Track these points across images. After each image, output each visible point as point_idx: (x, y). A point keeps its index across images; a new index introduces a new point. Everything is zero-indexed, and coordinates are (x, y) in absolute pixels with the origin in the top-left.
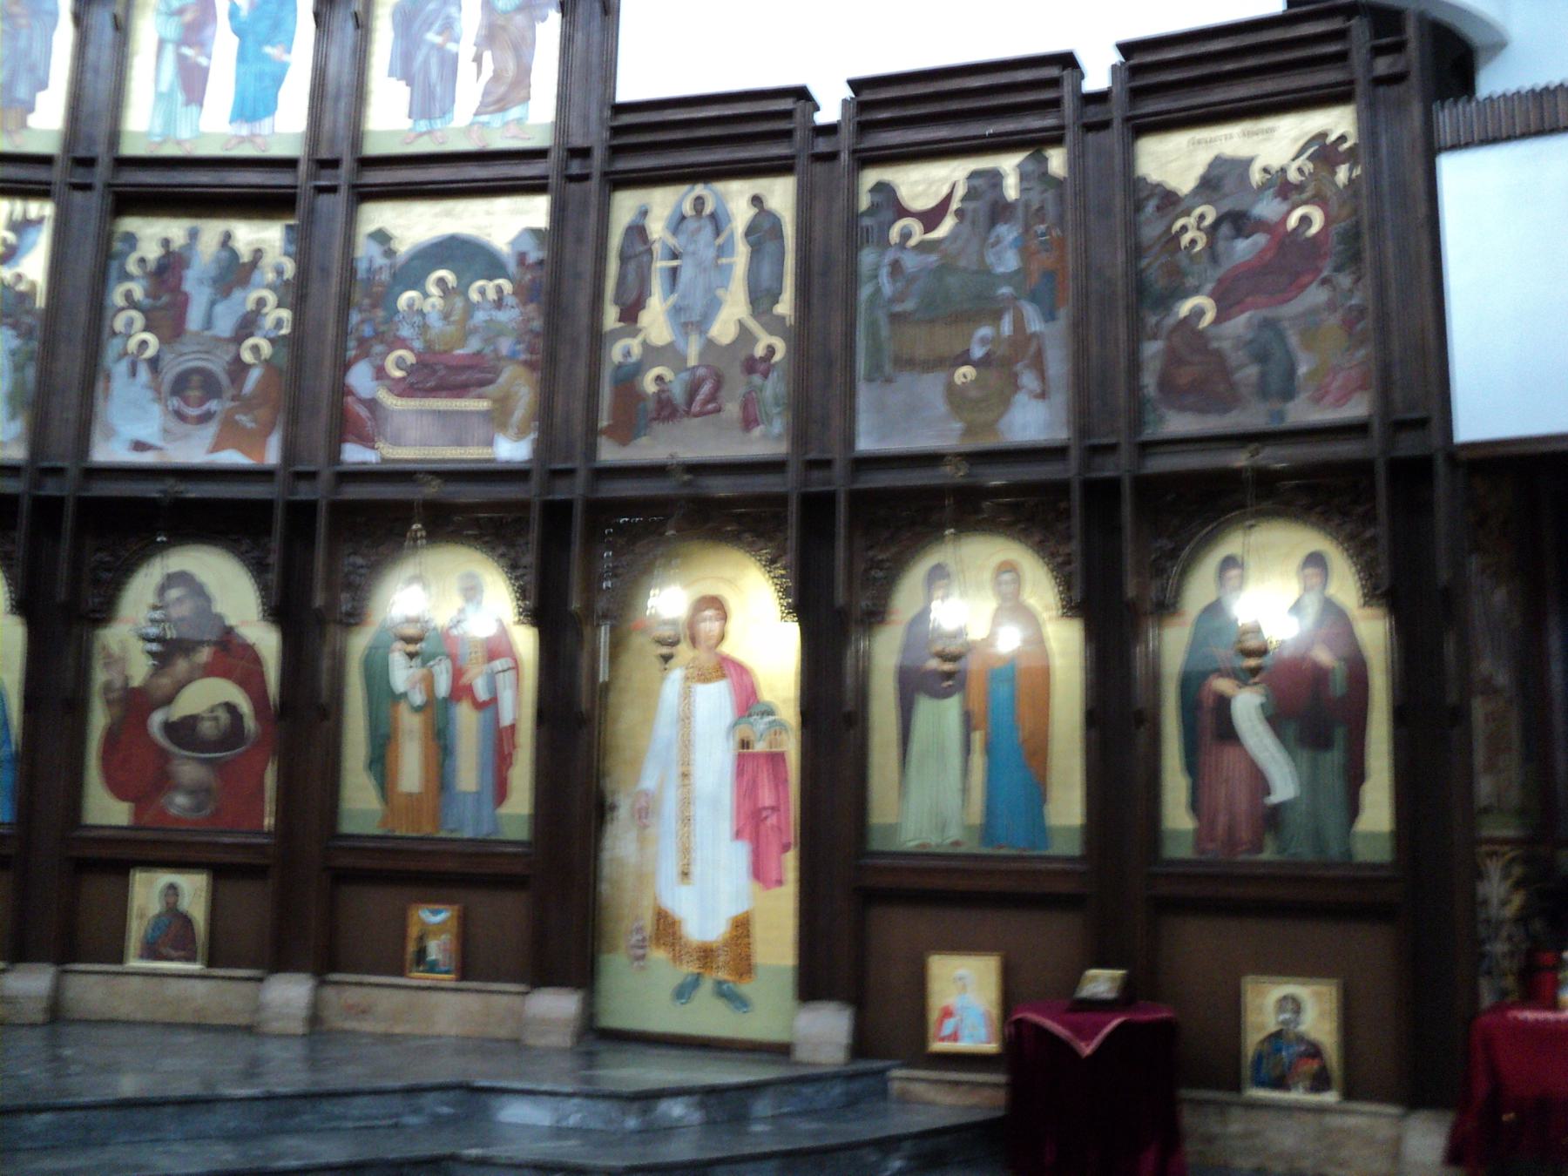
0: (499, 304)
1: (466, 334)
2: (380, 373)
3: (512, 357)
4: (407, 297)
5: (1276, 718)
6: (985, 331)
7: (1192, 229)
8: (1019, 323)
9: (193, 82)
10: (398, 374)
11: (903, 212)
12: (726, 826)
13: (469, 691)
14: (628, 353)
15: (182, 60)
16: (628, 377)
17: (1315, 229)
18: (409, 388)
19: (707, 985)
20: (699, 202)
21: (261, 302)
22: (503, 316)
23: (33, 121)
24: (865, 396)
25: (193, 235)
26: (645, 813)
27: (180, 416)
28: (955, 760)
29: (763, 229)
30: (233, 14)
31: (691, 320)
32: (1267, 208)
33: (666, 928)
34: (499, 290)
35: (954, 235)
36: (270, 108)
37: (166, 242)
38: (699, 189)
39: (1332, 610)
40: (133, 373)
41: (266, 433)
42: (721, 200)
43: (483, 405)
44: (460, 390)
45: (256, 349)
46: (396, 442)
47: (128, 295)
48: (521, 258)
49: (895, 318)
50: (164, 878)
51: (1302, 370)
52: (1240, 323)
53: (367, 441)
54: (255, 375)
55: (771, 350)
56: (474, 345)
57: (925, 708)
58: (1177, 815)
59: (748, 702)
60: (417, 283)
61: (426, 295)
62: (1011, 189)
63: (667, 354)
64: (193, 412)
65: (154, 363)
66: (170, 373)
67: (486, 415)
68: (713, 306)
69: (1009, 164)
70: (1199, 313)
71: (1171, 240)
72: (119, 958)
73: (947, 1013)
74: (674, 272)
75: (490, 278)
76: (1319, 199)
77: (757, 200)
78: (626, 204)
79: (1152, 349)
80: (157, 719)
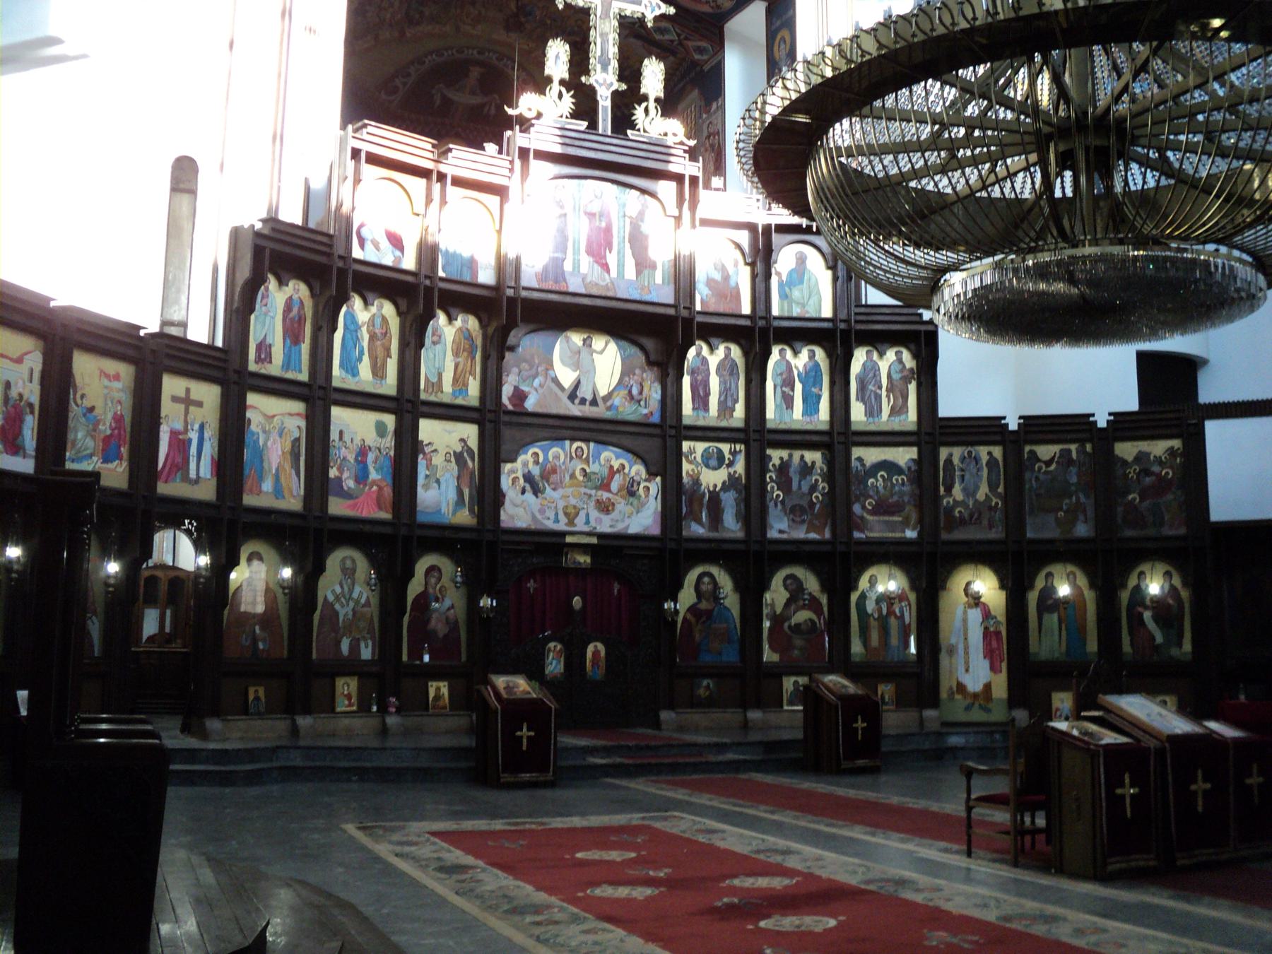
0: (903, 484)
1: (892, 495)
2: (864, 507)
3: (909, 501)
4: (871, 481)
5: (1156, 619)
6: (1067, 501)
7: (1132, 473)
8: (1078, 499)
9: (788, 401)
10: (870, 508)
11: (1039, 460)
12: (981, 655)
13: (894, 612)
14: (948, 502)
15: (783, 393)
16: (949, 511)
17: (1170, 476)
18: (874, 512)
19: (977, 705)
20: (970, 453)
21: (817, 481)
22: (905, 489)
23: (735, 414)
24: (1029, 520)
25: (791, 456)
26: (952, 651)
27: (793, 520)
28: (1056, 633)
29: (992, 462)
30: (799, 375)
31: (970, 492)
32: (1156, 469)
33: (961, 688)
34: (903, 480)
35: (1056, 469)
36: (817, 411)
37: (781, 459)
38: (970, 448)
39: (1173, 588)
40: (776, 505)
41: (826, 524)
42: (977, 453)
43: (900, 519)
44: (892, 514)
45: (817, 497)
46: (871, 531)
47: (770, 477)
48: (909, 468)
49: (1038, 495)
50: (793, 679)
51: (1166, 518)
52: (1147, 503)
53: (862, 531)
54: (818, 506)
55: (997, 504)
56: (895, 498)
57: (1046, 617)
58: (1127, 647)
59: (987, 614)
60: (875, 476)
61: (877, 480)
62: (1074, 455)
63: (963, 503)
64: (798, 519)
65: (783, 502)
66: (789, 505)
67: (901, 522)
68: (977, 488)
69: (1073, 447)
70: (1134, 499)
71: (1126, 475)
72: (782, 707)
73: (1057, 710)
74: (963, 477)
75: (899, 475)
76: (1171, 467)
77: (990, 453)
78: (944, 453)
79: (1120, 509)
80: (786, 625)
